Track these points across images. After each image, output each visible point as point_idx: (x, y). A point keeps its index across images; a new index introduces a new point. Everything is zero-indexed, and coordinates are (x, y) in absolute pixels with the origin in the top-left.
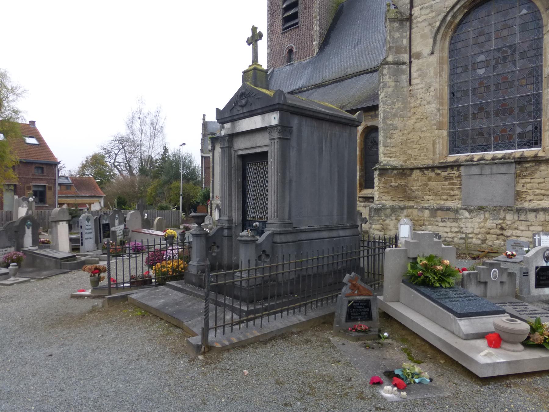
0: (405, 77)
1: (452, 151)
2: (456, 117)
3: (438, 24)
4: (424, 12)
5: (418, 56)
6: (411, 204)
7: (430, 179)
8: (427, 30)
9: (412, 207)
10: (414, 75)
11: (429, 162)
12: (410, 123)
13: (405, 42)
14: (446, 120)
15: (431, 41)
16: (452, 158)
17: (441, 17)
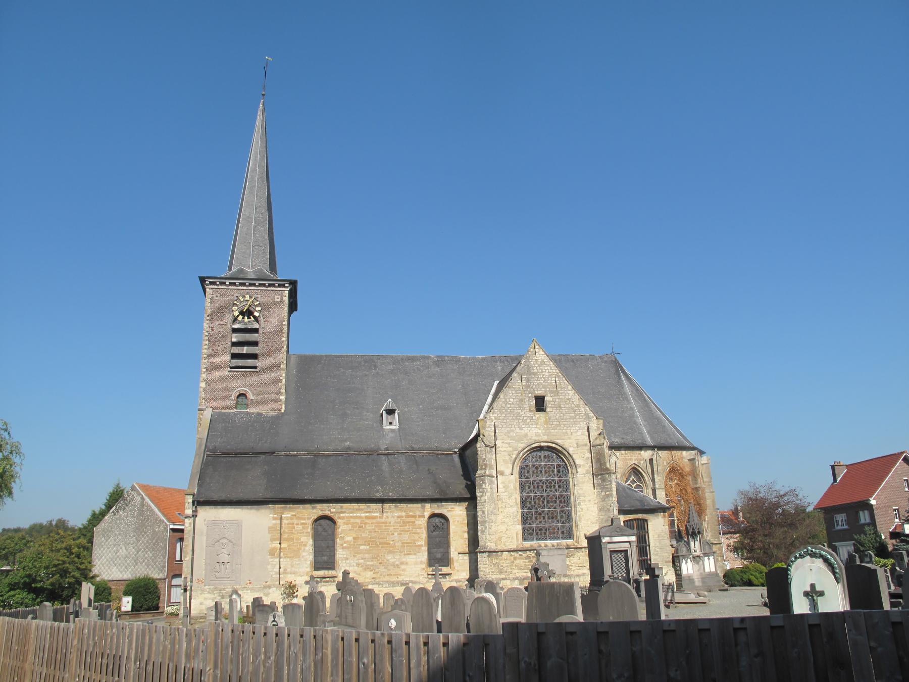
0: (495, 486)
1: (524, 540)
2: (525, 518)
3: (514, 456)
4: (504, 445)
5: (502, 474)
6: (503, 576)
7: (515, 559)
8: (507, 458)
9: (505, 579)
10: (500, 486)
11: (514, 547)
12: (500, 517)
13: (493, 462)
14: (519, 518)
15: (511, 466)
16: (528, 544)
17: (516, 452)
